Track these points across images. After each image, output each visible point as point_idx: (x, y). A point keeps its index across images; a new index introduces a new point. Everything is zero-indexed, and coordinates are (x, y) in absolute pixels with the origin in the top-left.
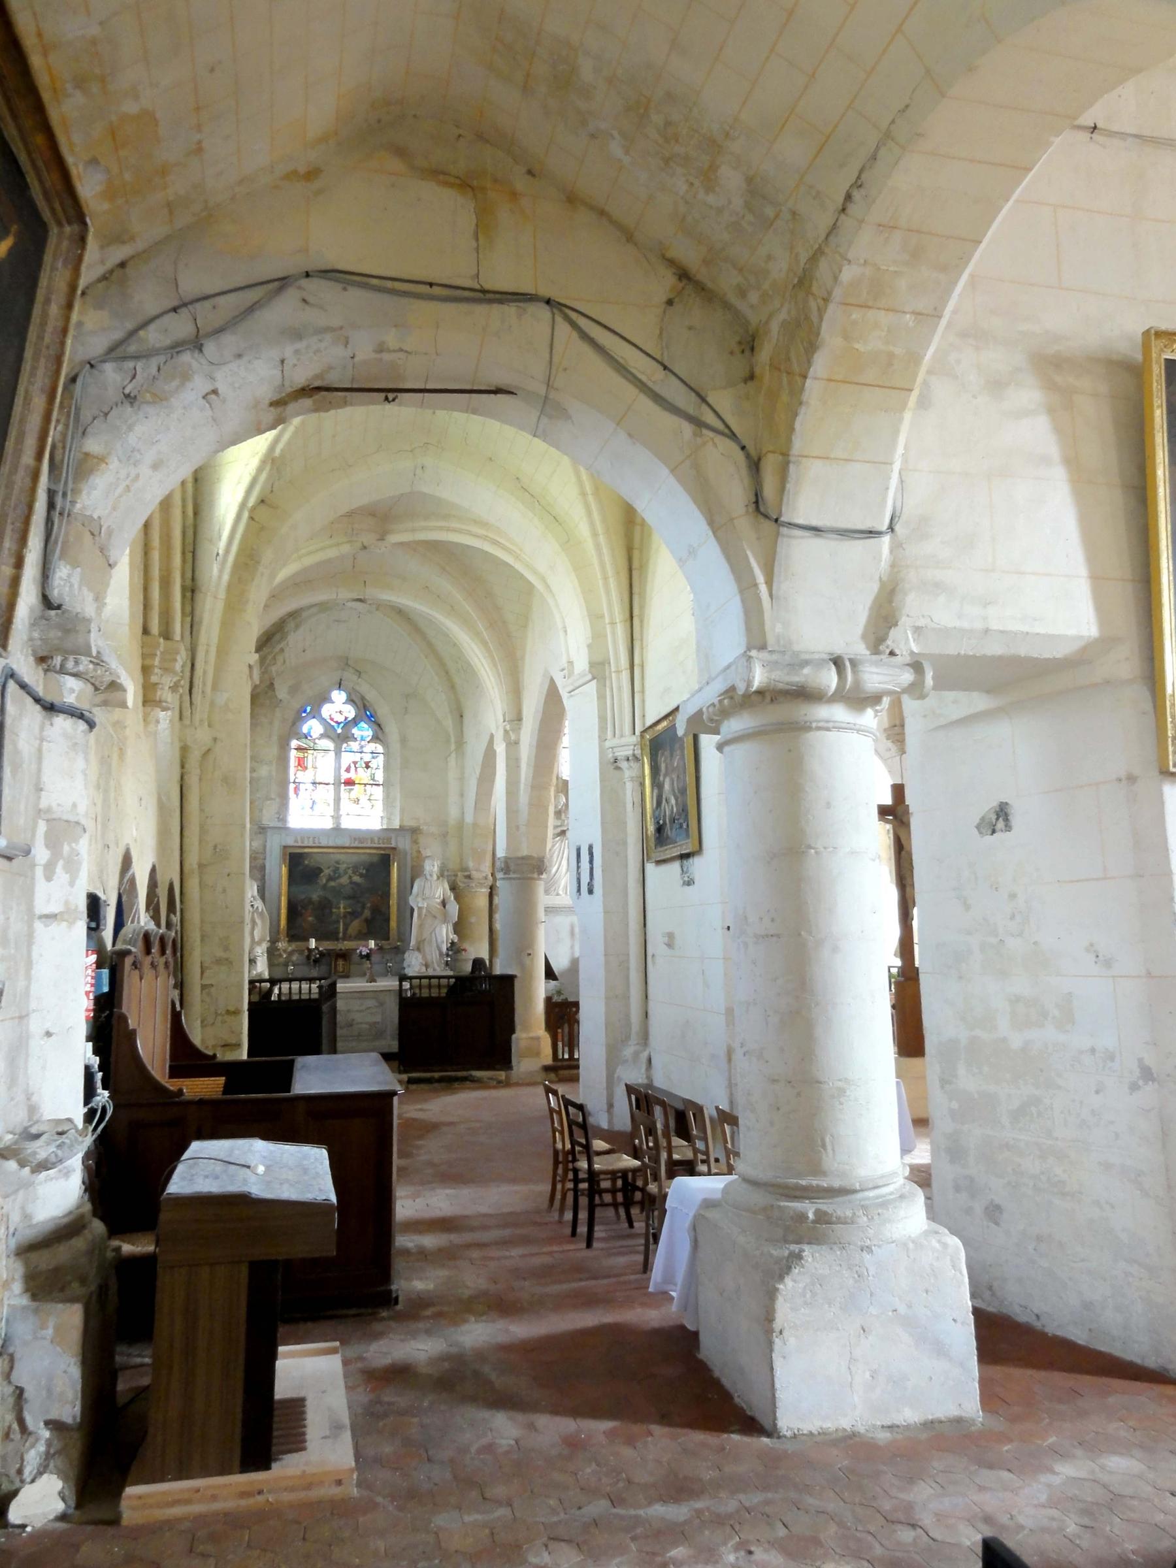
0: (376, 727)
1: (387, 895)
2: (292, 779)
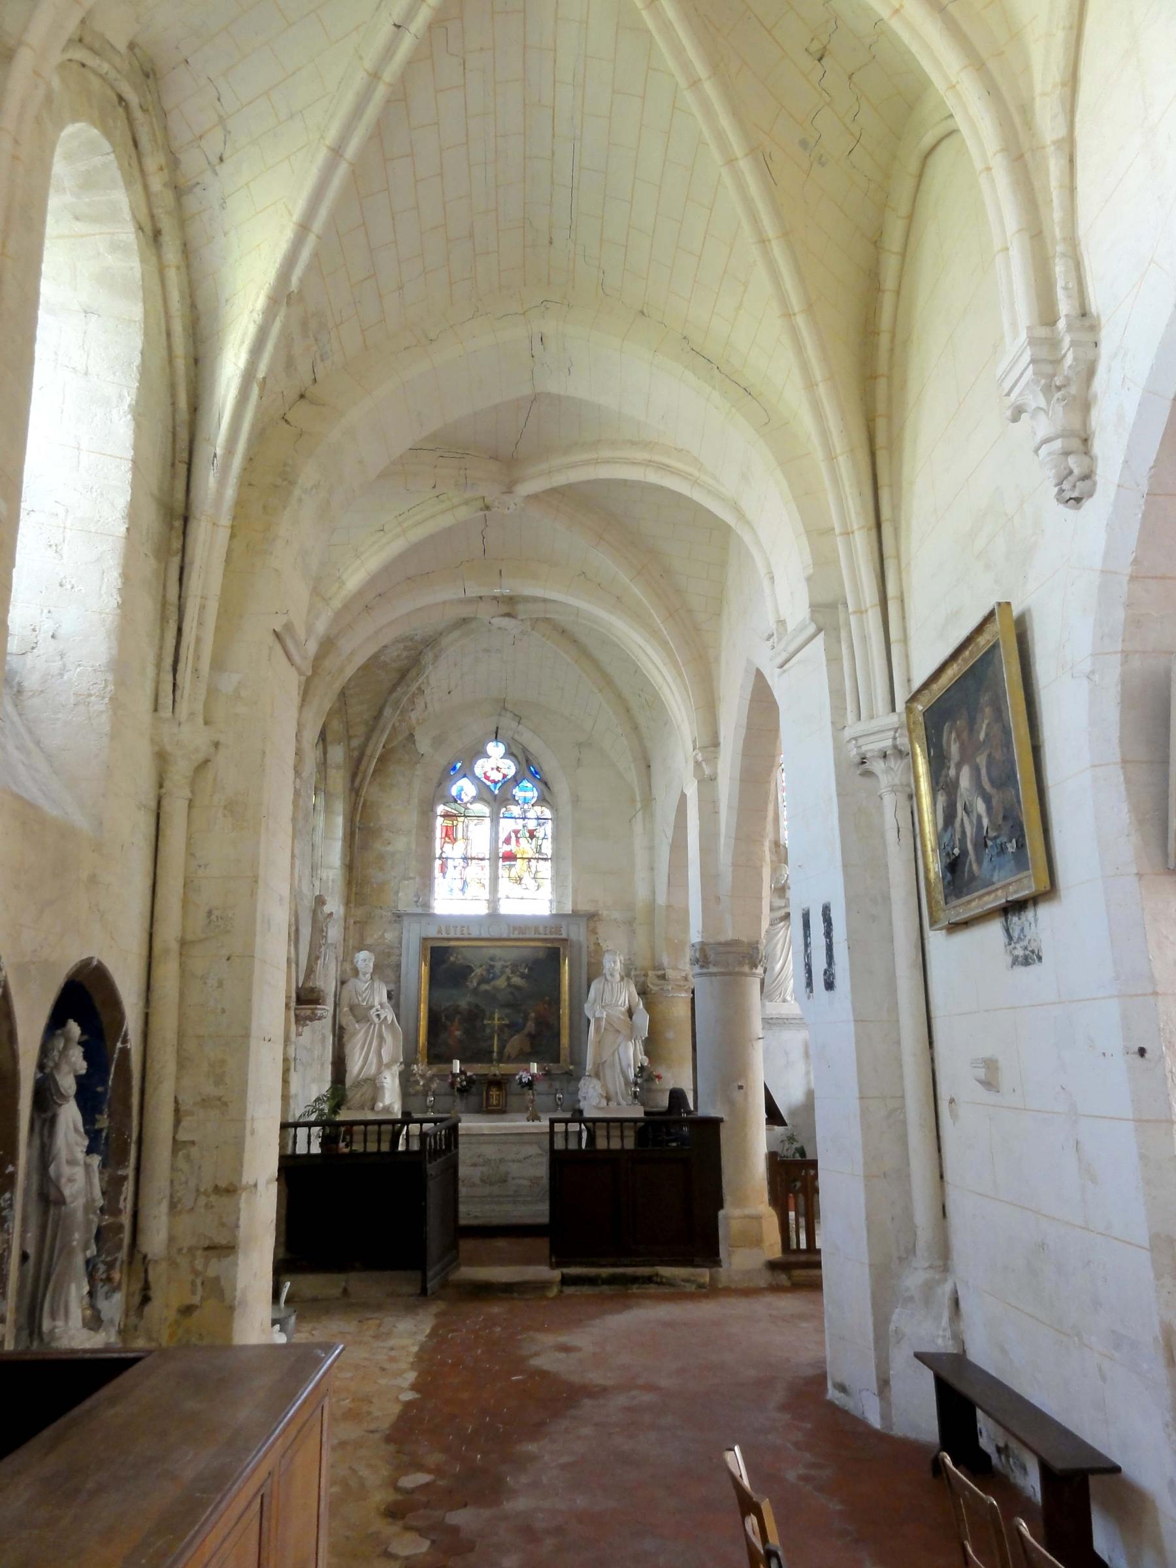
0: (542, 786)
1: (557, 1001)
2: (438, 853)
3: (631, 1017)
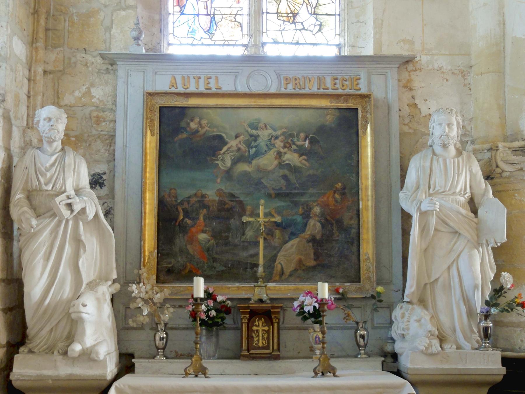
1: (351, 191)
3: (475, 212)
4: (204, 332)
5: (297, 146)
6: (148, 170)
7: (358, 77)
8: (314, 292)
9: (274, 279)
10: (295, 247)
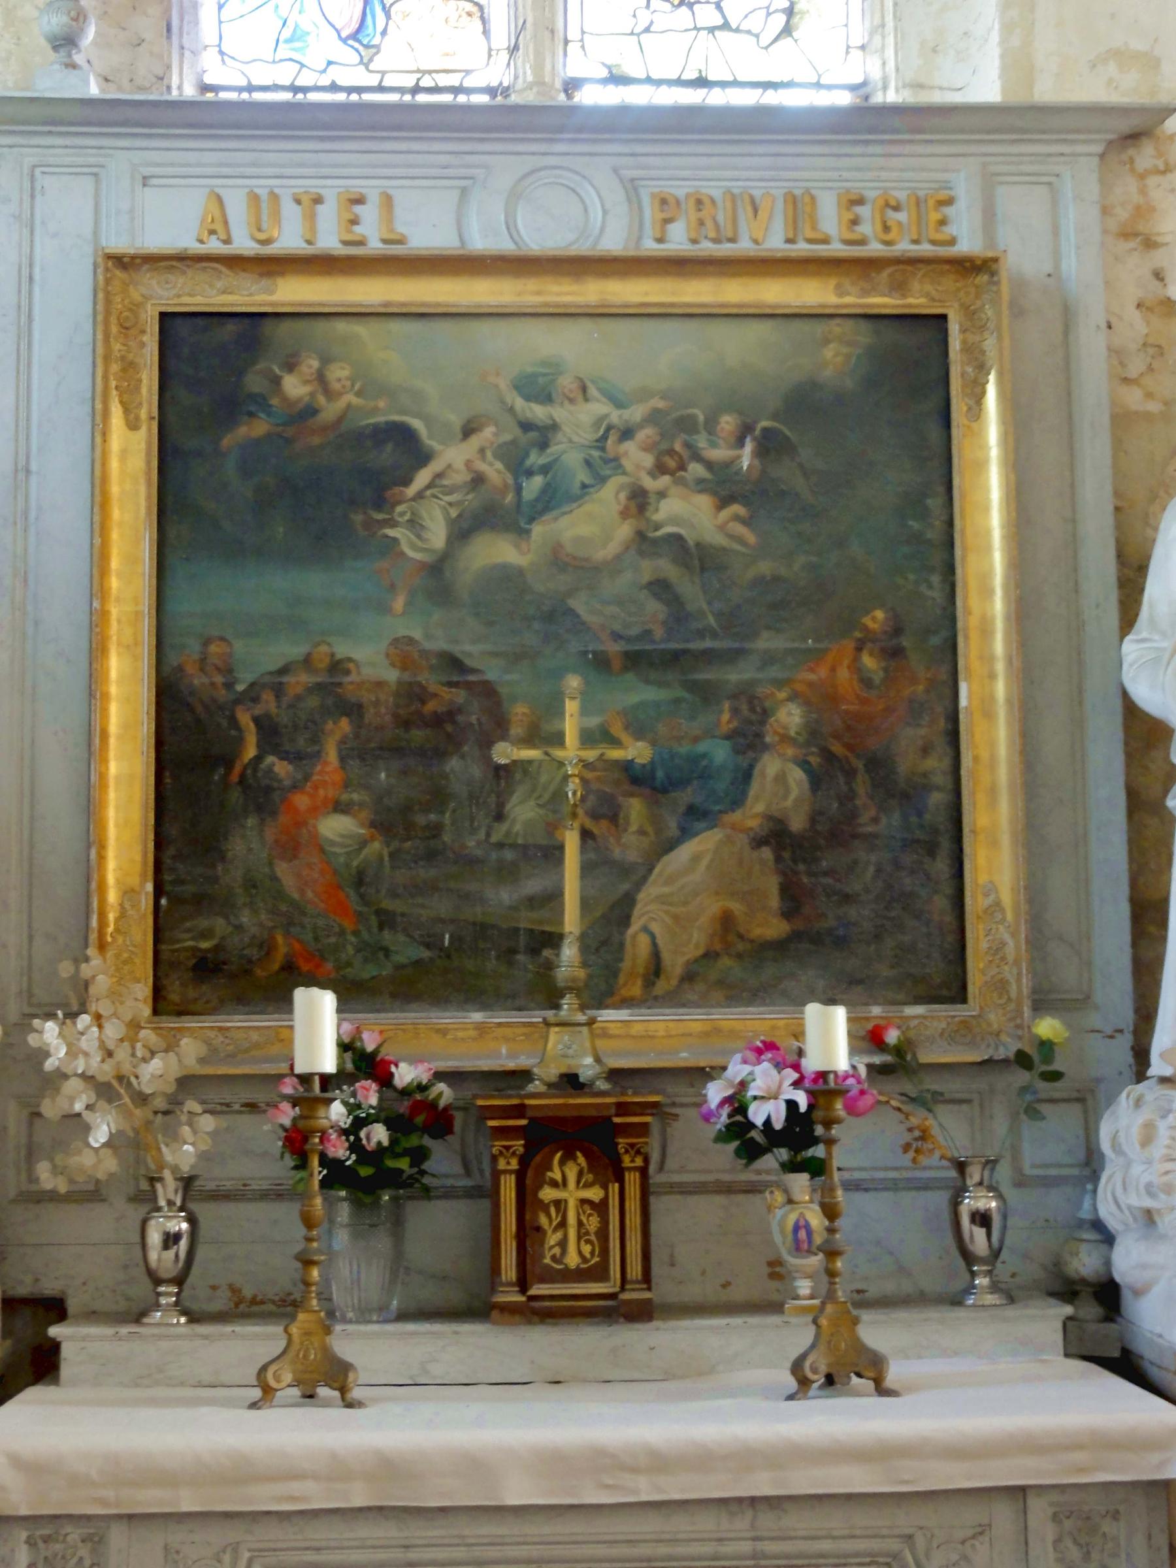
1: (929, 640)
4: (344, 1211)
5: (709, 465)
6: (115, 563)
7: (943, 195)
8: (788, 1044)
9: (624, 992)
10: (705, 862)
